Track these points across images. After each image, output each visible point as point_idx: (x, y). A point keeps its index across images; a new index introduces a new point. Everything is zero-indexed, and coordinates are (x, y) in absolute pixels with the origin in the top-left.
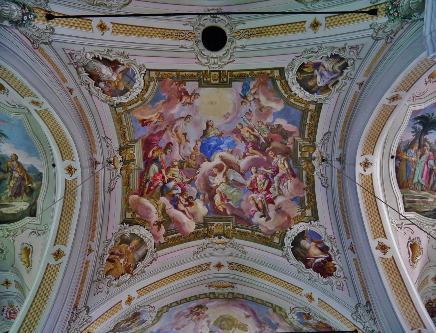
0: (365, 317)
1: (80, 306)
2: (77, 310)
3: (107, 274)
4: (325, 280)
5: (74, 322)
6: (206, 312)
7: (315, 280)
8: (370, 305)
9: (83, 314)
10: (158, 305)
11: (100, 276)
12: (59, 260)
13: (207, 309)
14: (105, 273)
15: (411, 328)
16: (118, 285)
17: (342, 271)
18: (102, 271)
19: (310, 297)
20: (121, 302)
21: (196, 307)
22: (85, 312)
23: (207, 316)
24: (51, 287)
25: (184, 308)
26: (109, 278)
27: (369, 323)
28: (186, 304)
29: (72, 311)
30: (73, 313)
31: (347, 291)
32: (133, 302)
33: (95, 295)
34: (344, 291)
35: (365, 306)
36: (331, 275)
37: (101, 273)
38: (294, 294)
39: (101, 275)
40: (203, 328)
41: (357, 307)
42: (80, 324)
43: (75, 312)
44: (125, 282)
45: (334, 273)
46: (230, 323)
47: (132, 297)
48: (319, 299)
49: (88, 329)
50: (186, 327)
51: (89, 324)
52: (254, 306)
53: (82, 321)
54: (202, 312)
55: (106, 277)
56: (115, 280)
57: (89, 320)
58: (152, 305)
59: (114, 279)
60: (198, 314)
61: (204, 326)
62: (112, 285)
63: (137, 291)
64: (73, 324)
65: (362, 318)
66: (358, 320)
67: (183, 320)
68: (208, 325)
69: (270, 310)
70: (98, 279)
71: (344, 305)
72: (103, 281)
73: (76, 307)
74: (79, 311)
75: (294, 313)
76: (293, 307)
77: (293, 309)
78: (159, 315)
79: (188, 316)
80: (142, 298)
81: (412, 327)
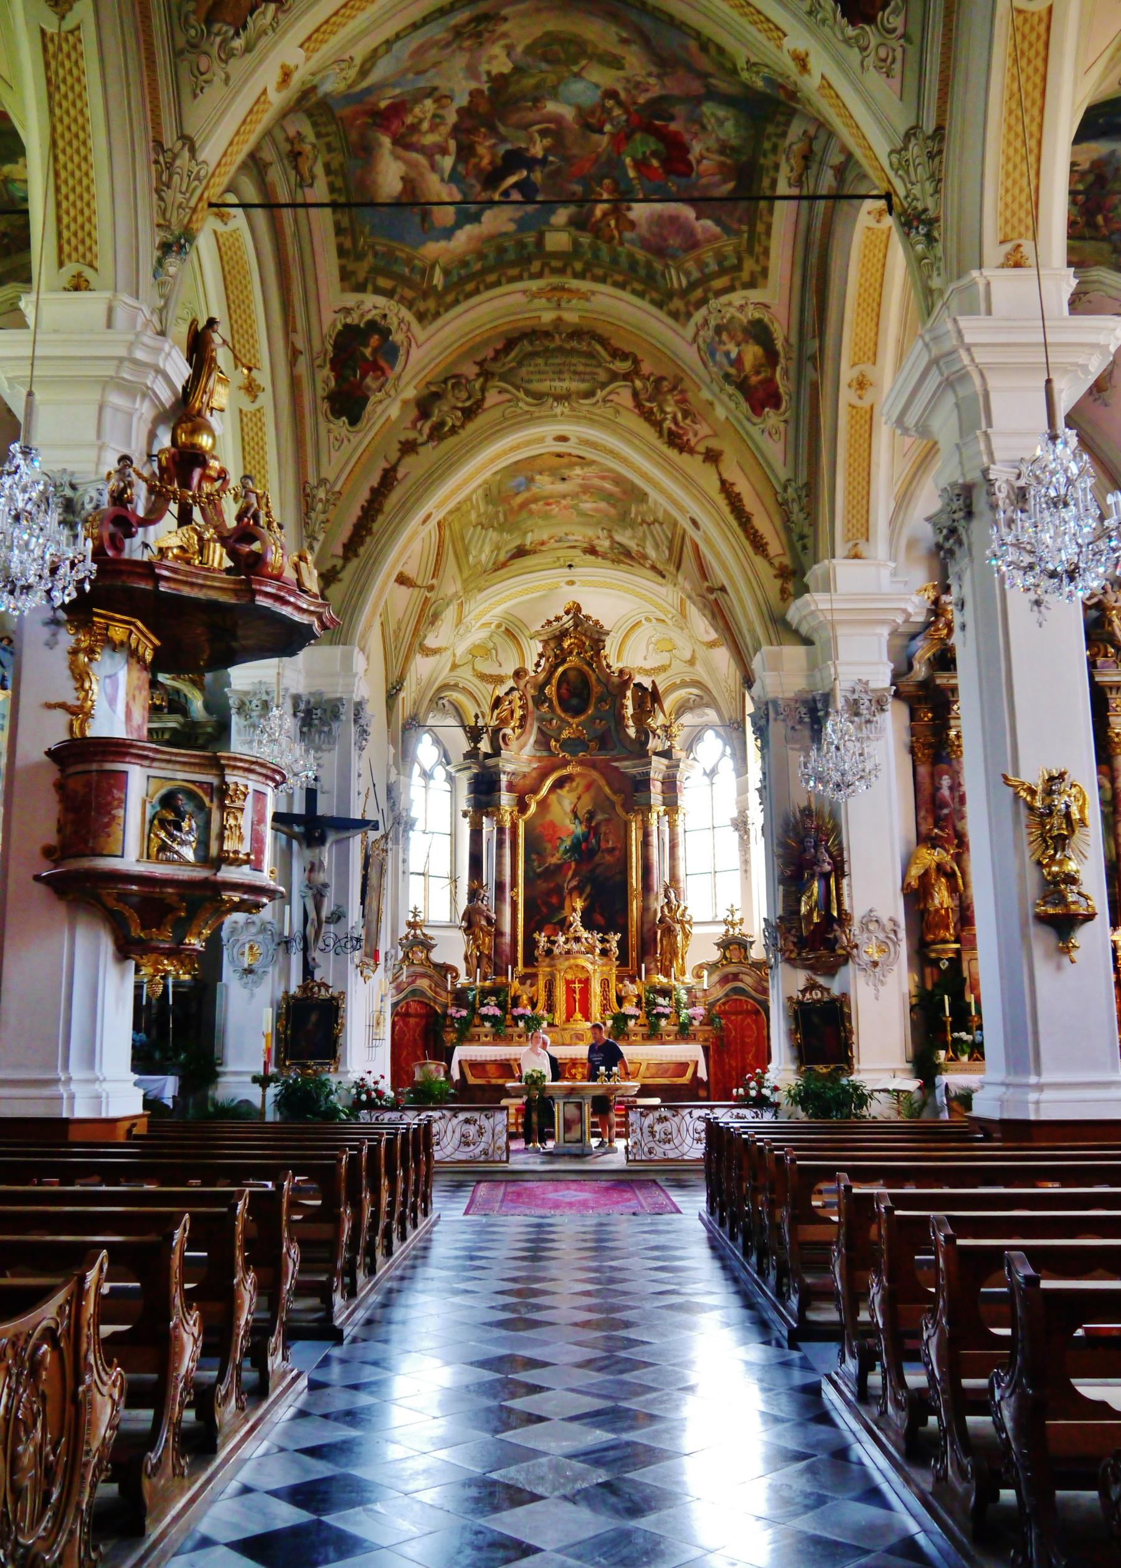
0: (920, 168)
1: (169, 139)
2: (164, 151)
3: (209, 21)
4: (850, 31)
5: (169, 187)
6: (505, 27)
7: (824, 21)
8: (942, 140)
9: (183, 161)
10: (359, 53)
11: (193, 32)
12: (69, 16)
13: (505, 19)
14: (203, 16)
15: (1001, 237)
16: (248, 49)
17: (903, 15)
18: (194, 12)
19: (802, 61)
20: (264, 92)
21: (469, 22)
22: (186, 154)
23: (505, 35)
24: (82, 112)
25: (436, 31)
26: (218, 34)
27: (923, 189)
28: (442, 20)
29: (153, 157)
30: (156, 162)
31: (898, 80)
32: (296, 79)
33: (195, 96)
34: (890, 80)
35: (929, 138)
36: (871, 20)
37: (192, 19)
38: (761, 37)
39: (193, 27)
40: (495, 62)
41: (909, 135)
42: (184, 189)
43: (161, 159)
44: (265, 33)
45: (880, 14)
46: (573, 50)
47: (292, 67)
48: (823, 77)
49: (206, 195)
50: (445, 65)
51: (204, 182)
52: (647, 24)
53: (186, 179)
54: (490, 28)
55: (209, 33)
56: (237, 34)
57: (202, 173)
58: (346, 57)
59: (231, 32)
60: (479, 35)
61: (496, 57)
62: (231, 54)
63: (301, 46)
64: (168, 195)
65: (911, 169)
66: (900, 172)
67: (433, 54)
68: (508, 55)
69: (692, 44)
70: (188, 42)
71: (880, 119)
72: (205, 46)
73: (158, 144)
74: (169, 154)
75: (758, 73)
76: (753, 59)
77: (755, 64)
78: (368, 66)
79: (448, 44)
80: (316, 56)
81: (1006, 235)
